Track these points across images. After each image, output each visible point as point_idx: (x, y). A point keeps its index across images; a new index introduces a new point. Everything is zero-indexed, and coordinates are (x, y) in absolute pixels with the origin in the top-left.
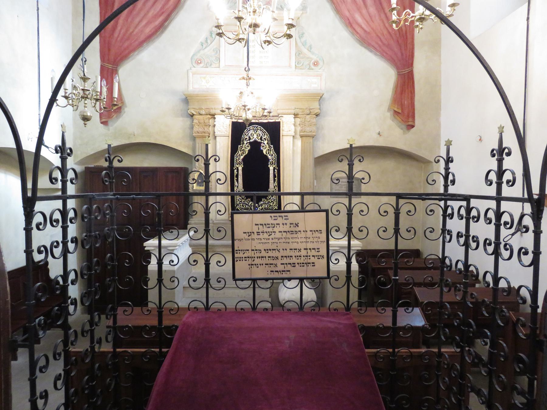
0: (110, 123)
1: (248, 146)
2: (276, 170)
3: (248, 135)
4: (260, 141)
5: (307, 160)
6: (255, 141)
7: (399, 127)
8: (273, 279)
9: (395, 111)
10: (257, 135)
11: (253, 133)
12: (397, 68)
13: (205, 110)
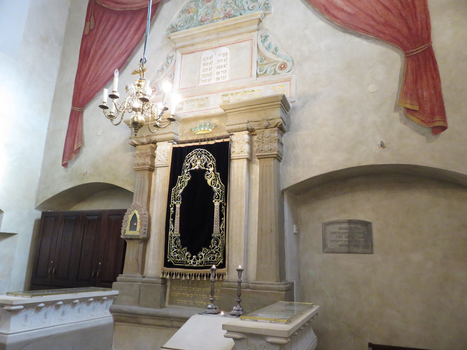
0: (69, 165)
1: (188, 176)
2: (223, 207)
3: (189, 161)
4: (204, 168)
5: (267, 191)
7: (417, 131)
10: (201, 161)
11: (197, 158)
12: (404, 49)
13: (147, 137)
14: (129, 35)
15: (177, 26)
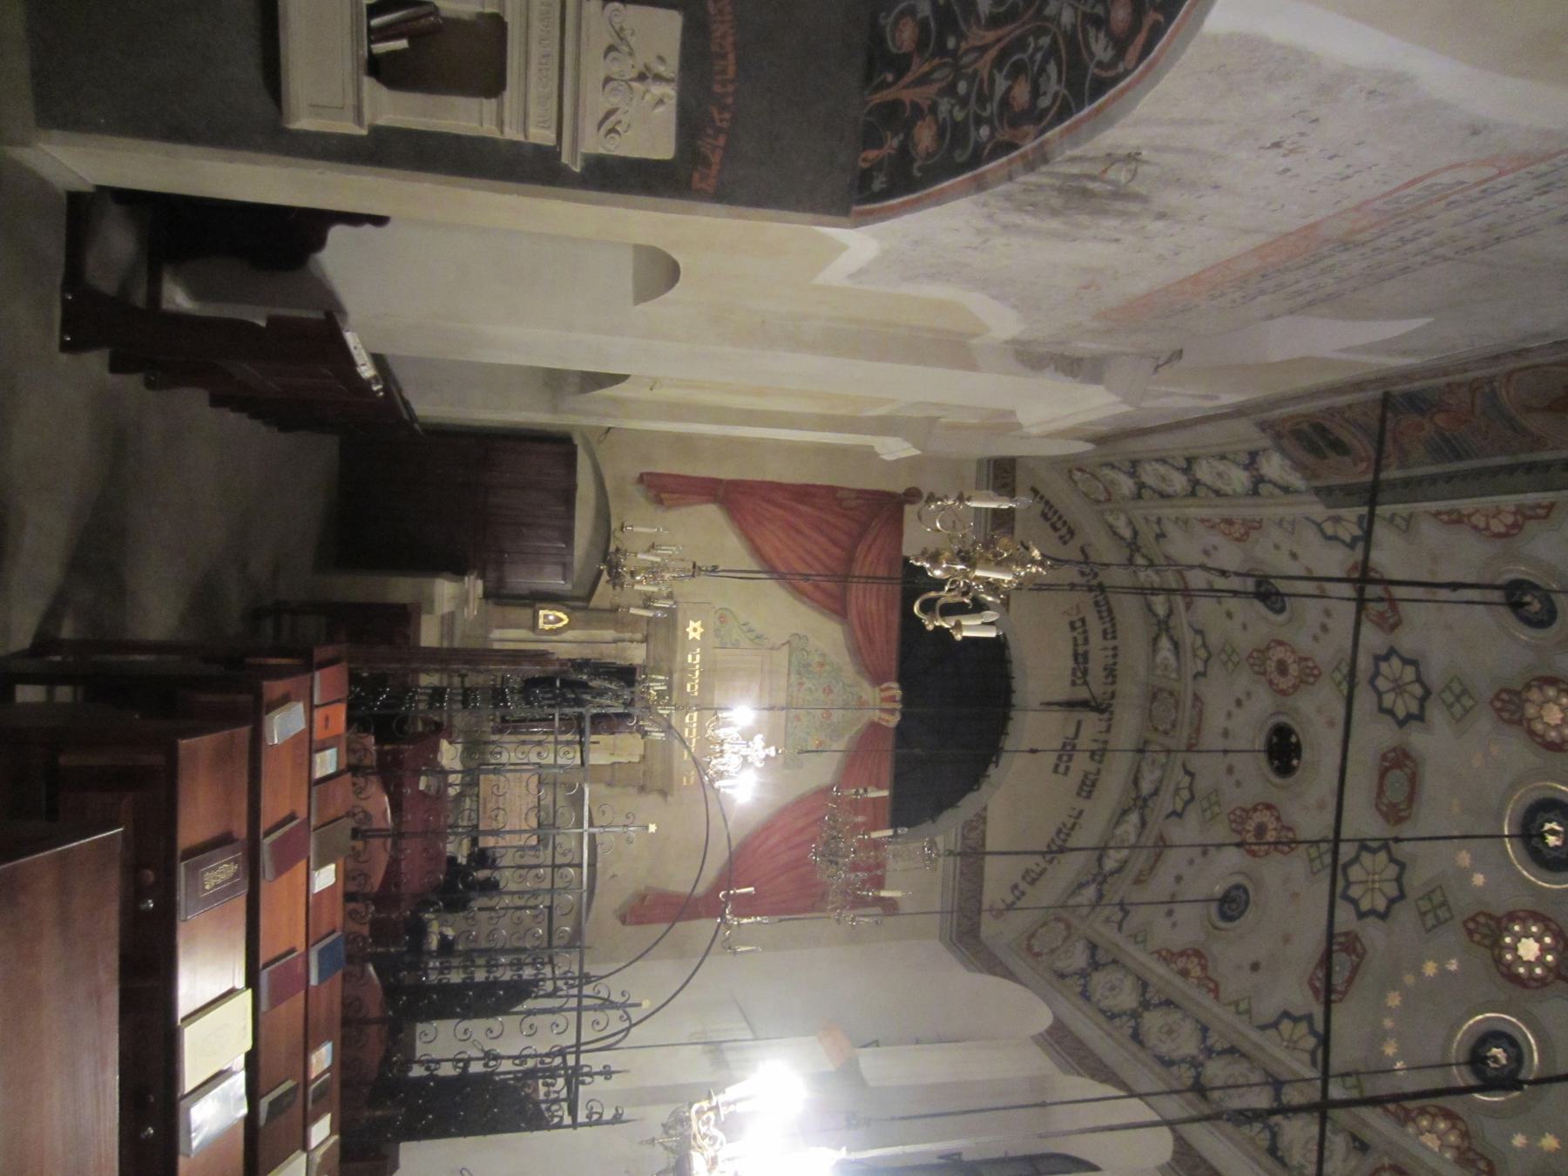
9: (643, 897)
15: (803, 649)
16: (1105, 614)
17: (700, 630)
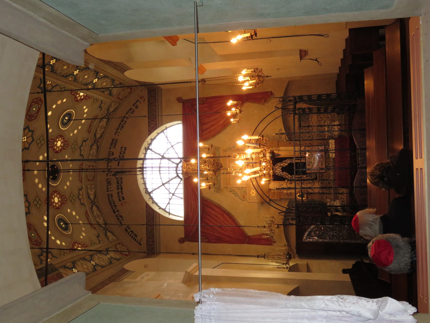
6: (281, 169)
8: (325, 161)
14: (214, 213)
16: (112, 203)
17: (251, 193)
